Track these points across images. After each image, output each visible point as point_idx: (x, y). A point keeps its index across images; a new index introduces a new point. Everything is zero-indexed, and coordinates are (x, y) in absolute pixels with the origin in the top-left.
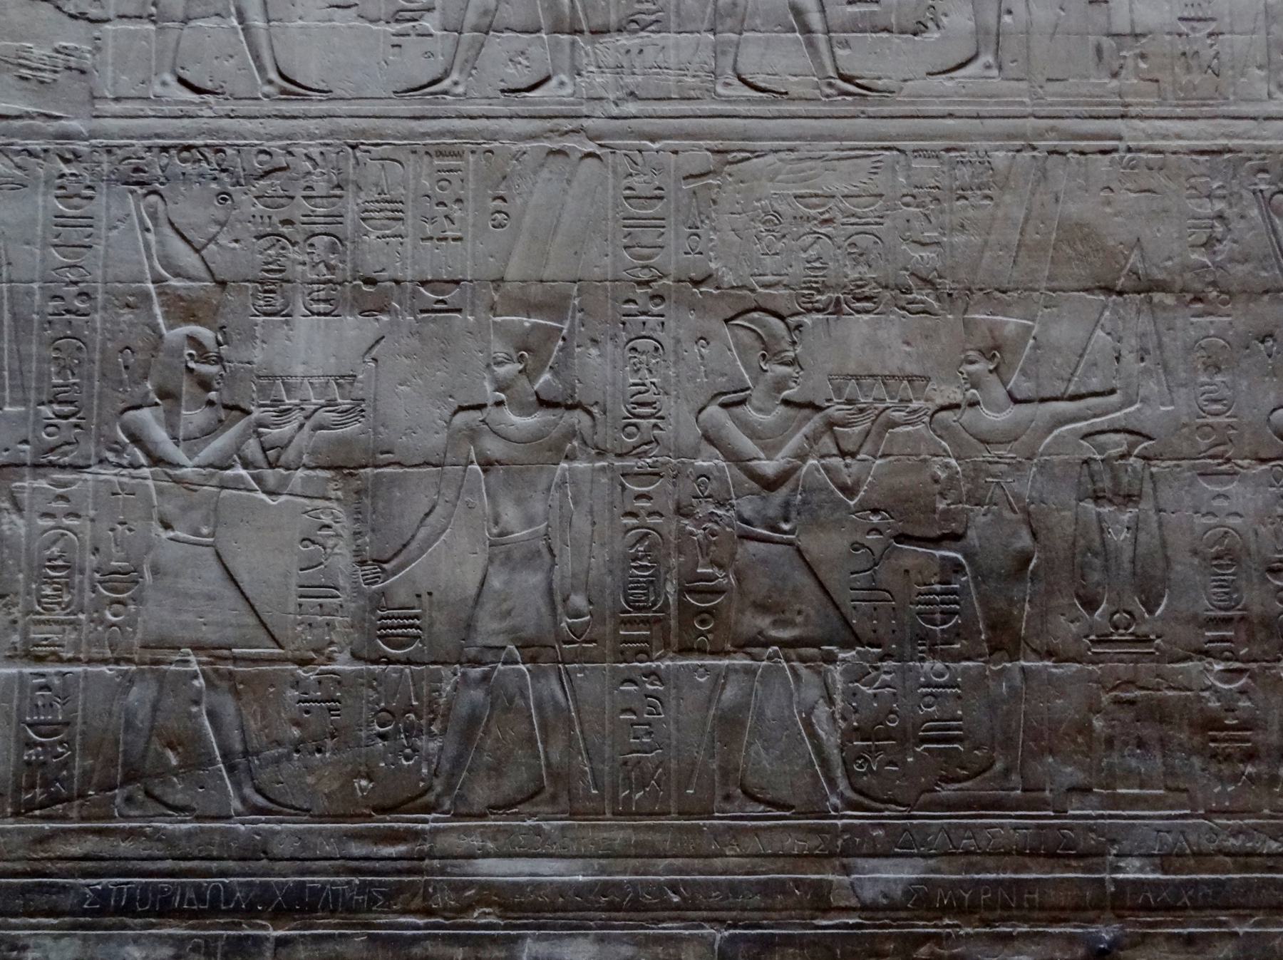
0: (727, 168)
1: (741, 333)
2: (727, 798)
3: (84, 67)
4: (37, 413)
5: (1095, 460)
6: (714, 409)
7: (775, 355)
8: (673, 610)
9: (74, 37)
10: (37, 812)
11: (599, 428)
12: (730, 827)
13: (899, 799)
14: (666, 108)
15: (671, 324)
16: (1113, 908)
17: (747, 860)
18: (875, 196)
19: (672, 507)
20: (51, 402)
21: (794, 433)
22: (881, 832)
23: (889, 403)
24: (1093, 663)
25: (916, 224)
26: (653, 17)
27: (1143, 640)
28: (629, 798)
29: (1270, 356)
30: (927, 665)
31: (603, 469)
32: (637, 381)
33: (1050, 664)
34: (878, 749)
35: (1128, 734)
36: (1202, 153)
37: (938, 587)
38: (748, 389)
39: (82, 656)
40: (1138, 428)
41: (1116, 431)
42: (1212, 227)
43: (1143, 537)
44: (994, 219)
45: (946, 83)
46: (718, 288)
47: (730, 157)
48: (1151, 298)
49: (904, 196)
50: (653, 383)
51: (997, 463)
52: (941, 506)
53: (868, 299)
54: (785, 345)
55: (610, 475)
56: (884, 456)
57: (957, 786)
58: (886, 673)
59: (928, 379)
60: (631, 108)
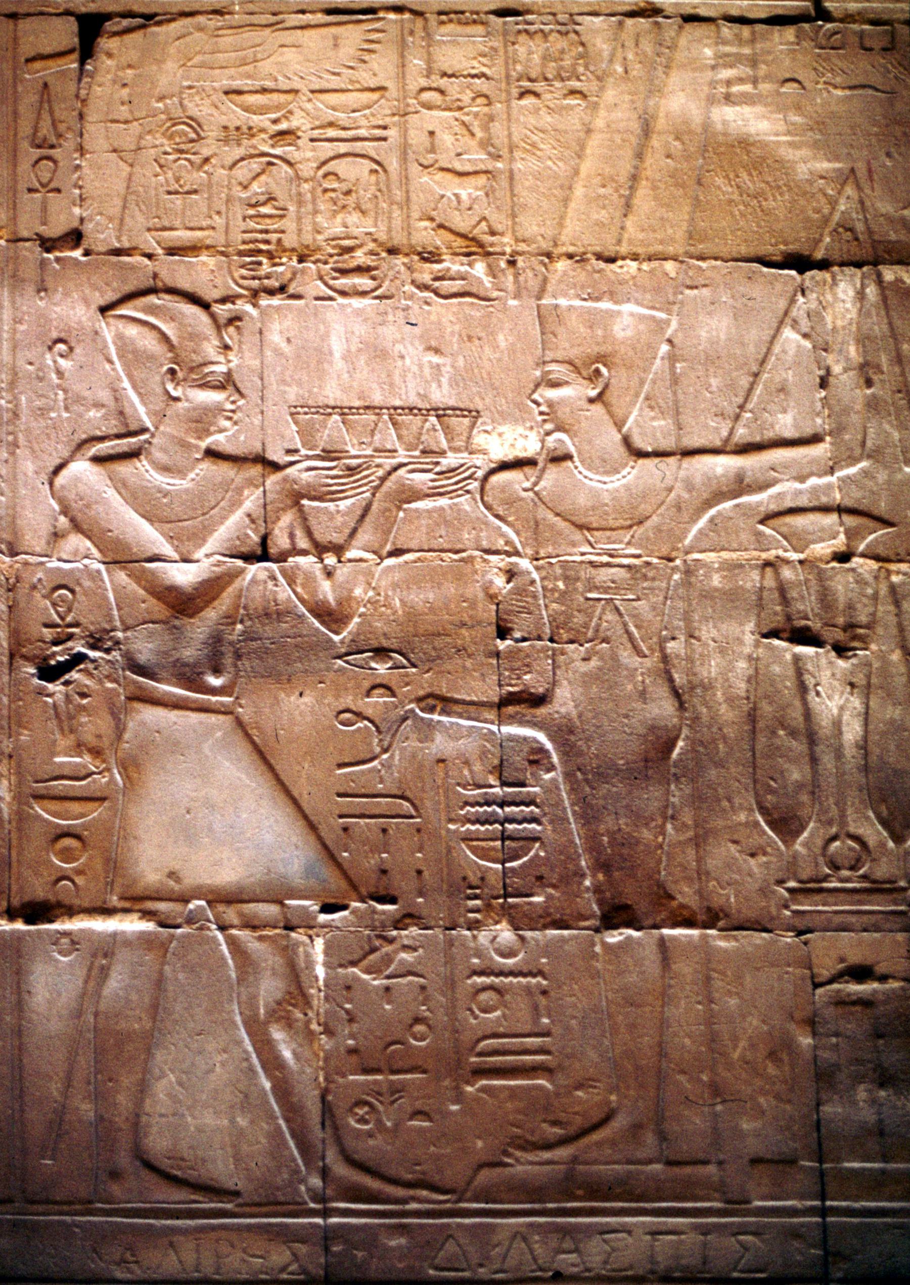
5: (787, 562)
7: (192, 370)
18: (372, 90)
22: (403, 1241)
23: (402, 456)
25: (446, 139)
30: (483, 937)
38: (144, 430)
41: (825, 509)
44: (589, 131)
48: (879, 275)
49: (423, 90)
51: (608, 565)
53: (360, 270)
56: (397, 552)
57: (547, 1155)
58: (405, 948)
59: (474, 415)
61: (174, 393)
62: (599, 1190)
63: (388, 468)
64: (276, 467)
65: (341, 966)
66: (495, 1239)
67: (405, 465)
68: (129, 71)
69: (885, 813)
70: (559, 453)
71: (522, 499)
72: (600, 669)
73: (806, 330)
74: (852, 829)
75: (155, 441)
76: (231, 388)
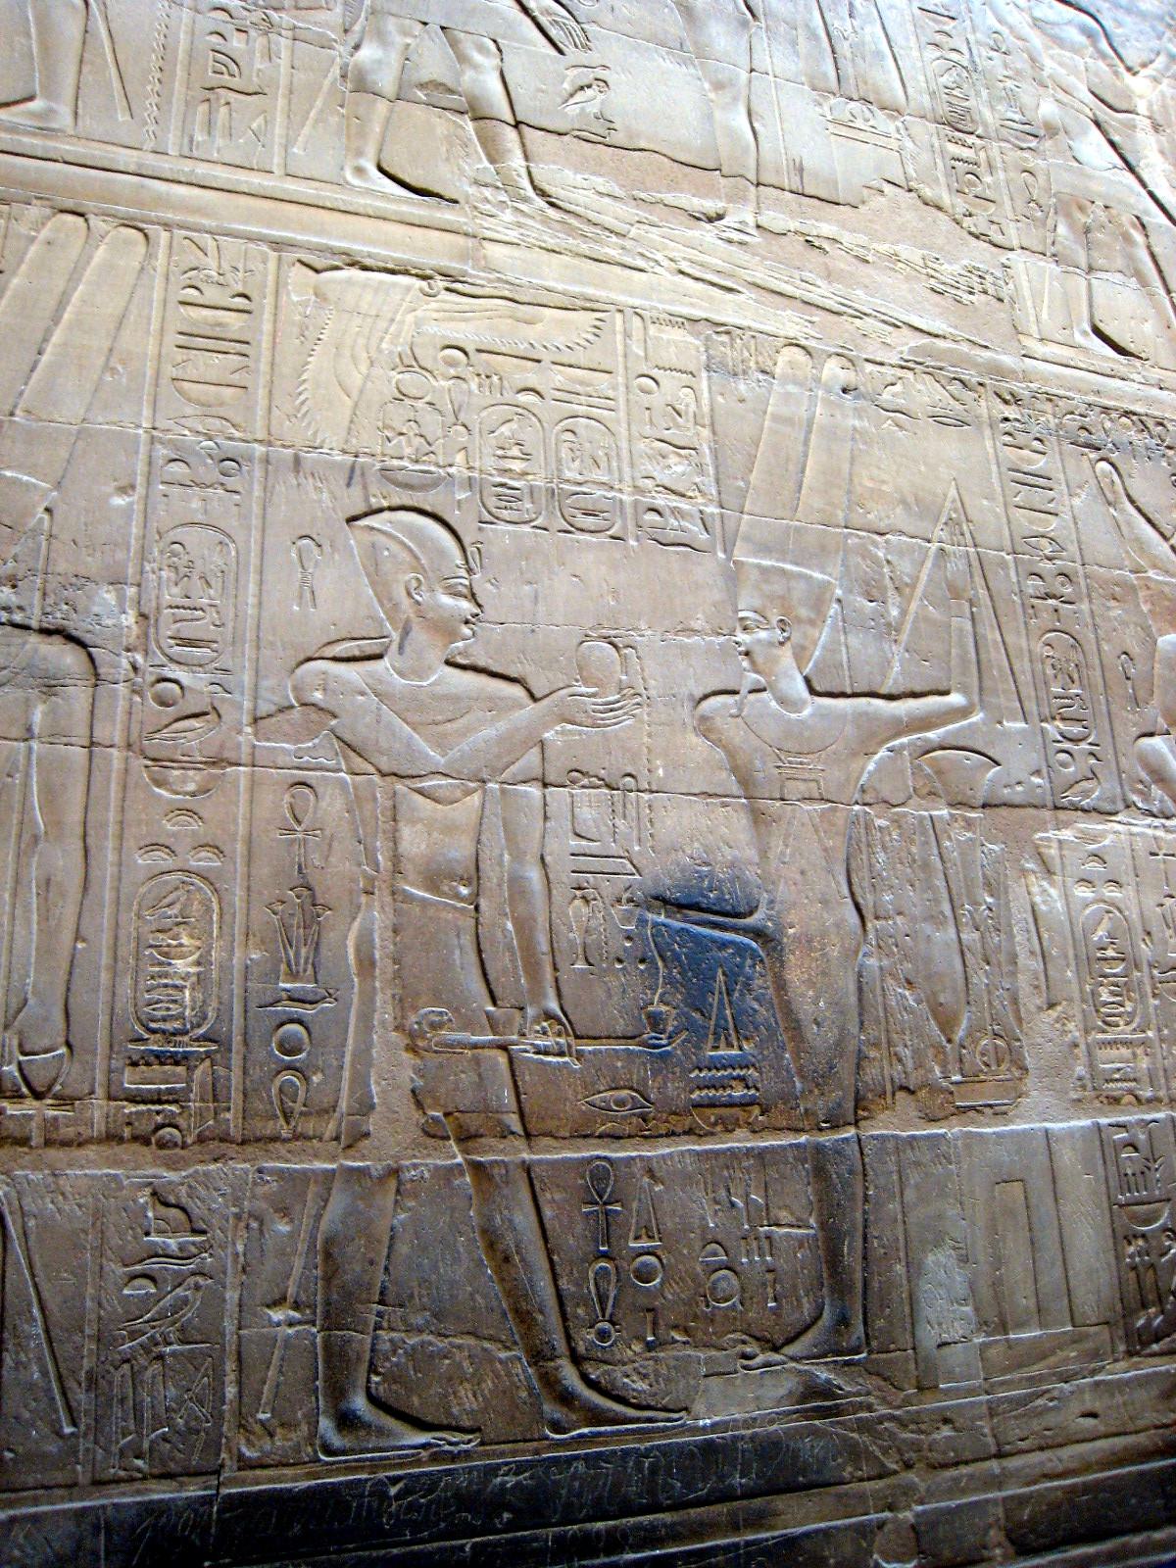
3: (1001, 295)
4: (1043, 731)
9: (980, 255)
10: (1155, 1347)
20: (1054, 718)
39: (1162, 1093)
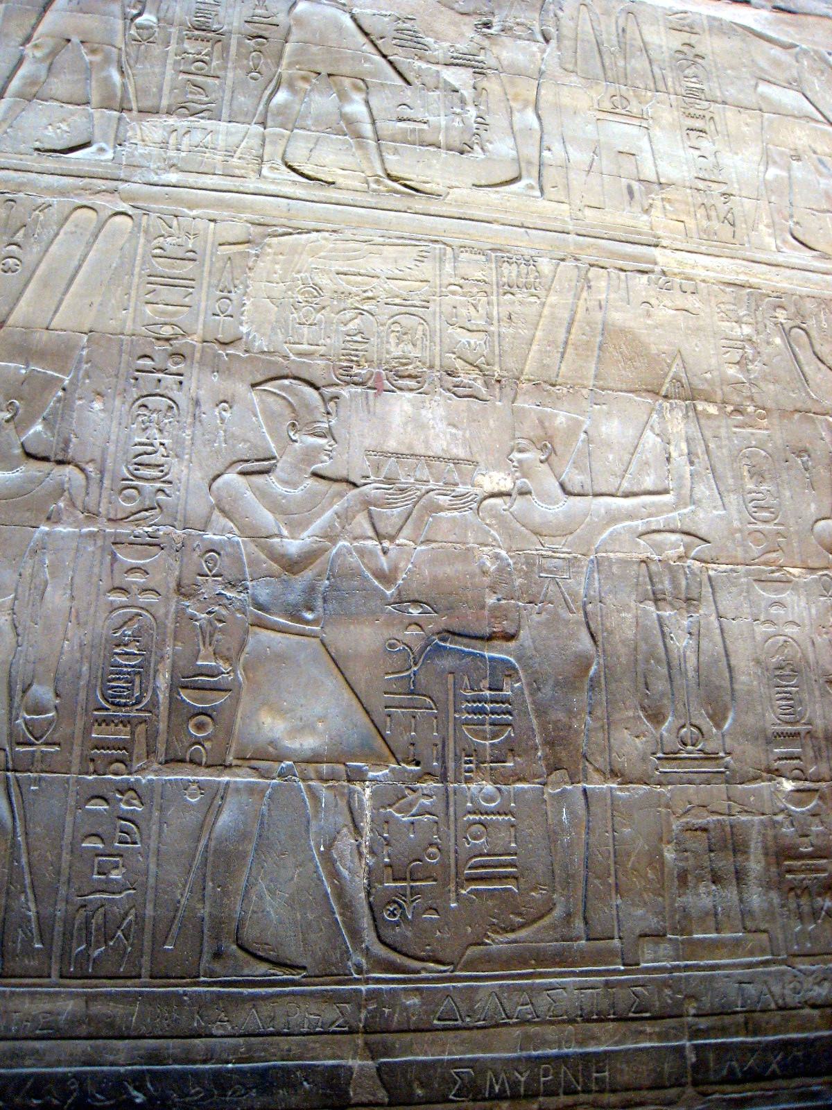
0: (267, 240)
1: (271, 399)
2: (218, 955)
6: (231, 477)
8: (163, 709)
11: (94, 488)
12: (219, 996)
13: (440, 955)
14: (208, 181)
15: (191, 384)
16: (695, 1084)
17: (241, 1040)
19: (173, 585)
21: (323, 511)
24: (660, 784)
26: (204, 107)
27: (710, 757)
28: (85, 955)
29: (806, 469)
31: (92, 535)
32: (144, 440)
33: (615, 786)
34: (414, 891)
35: (702, 868)
36: (730, 284)
37: (488, 693)
38: (274, 458)
40: (693, 529)
41: (673, 531)
42: (743, 348)
43: (705, 644)
45: (492, 195)
46: (246, 351)
47: (270, 230)
50: (162, 444)
52: (491, 600)
54: (319, 417)
55: (100, 543)
56: (427, 541)
57: (511, 936)
60: (173, 177)
61: (294, 438)
62: (542, 959)
63: (423, 491)
64: (355, 485)
65: (383, 807)
66: (478, 998)
67: (433, 490)
68: (280, 257)
69: (711, 712)
70: (523, 490)
71: (502, 516)
72: (547, 619)
73: (657, 431)
74: (694, 721)
75: (278, 465)
76: (330, 438)
